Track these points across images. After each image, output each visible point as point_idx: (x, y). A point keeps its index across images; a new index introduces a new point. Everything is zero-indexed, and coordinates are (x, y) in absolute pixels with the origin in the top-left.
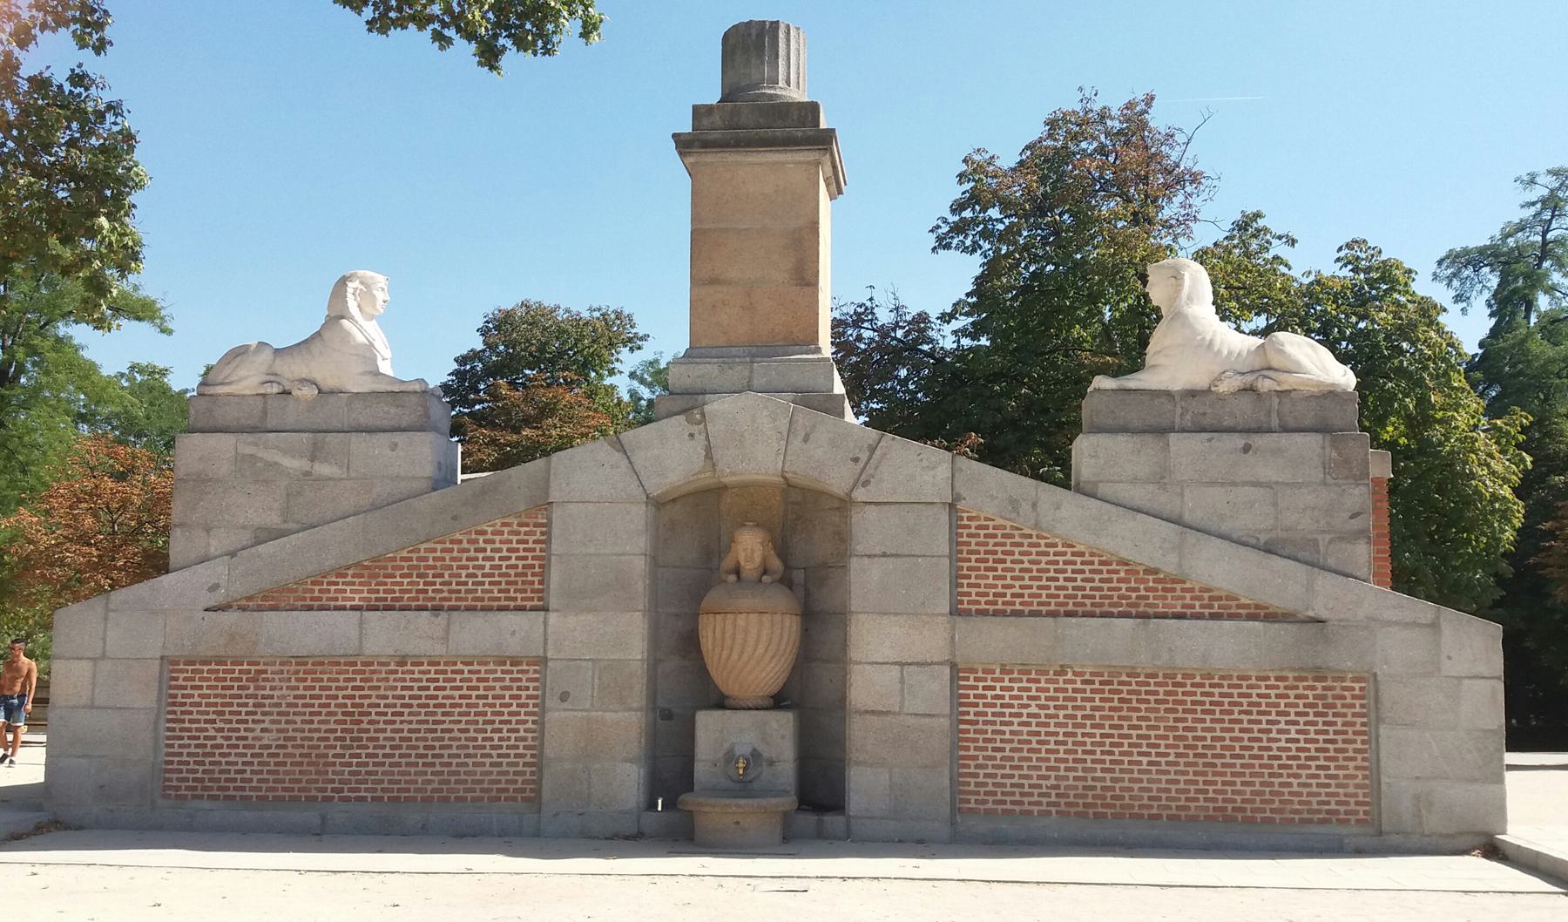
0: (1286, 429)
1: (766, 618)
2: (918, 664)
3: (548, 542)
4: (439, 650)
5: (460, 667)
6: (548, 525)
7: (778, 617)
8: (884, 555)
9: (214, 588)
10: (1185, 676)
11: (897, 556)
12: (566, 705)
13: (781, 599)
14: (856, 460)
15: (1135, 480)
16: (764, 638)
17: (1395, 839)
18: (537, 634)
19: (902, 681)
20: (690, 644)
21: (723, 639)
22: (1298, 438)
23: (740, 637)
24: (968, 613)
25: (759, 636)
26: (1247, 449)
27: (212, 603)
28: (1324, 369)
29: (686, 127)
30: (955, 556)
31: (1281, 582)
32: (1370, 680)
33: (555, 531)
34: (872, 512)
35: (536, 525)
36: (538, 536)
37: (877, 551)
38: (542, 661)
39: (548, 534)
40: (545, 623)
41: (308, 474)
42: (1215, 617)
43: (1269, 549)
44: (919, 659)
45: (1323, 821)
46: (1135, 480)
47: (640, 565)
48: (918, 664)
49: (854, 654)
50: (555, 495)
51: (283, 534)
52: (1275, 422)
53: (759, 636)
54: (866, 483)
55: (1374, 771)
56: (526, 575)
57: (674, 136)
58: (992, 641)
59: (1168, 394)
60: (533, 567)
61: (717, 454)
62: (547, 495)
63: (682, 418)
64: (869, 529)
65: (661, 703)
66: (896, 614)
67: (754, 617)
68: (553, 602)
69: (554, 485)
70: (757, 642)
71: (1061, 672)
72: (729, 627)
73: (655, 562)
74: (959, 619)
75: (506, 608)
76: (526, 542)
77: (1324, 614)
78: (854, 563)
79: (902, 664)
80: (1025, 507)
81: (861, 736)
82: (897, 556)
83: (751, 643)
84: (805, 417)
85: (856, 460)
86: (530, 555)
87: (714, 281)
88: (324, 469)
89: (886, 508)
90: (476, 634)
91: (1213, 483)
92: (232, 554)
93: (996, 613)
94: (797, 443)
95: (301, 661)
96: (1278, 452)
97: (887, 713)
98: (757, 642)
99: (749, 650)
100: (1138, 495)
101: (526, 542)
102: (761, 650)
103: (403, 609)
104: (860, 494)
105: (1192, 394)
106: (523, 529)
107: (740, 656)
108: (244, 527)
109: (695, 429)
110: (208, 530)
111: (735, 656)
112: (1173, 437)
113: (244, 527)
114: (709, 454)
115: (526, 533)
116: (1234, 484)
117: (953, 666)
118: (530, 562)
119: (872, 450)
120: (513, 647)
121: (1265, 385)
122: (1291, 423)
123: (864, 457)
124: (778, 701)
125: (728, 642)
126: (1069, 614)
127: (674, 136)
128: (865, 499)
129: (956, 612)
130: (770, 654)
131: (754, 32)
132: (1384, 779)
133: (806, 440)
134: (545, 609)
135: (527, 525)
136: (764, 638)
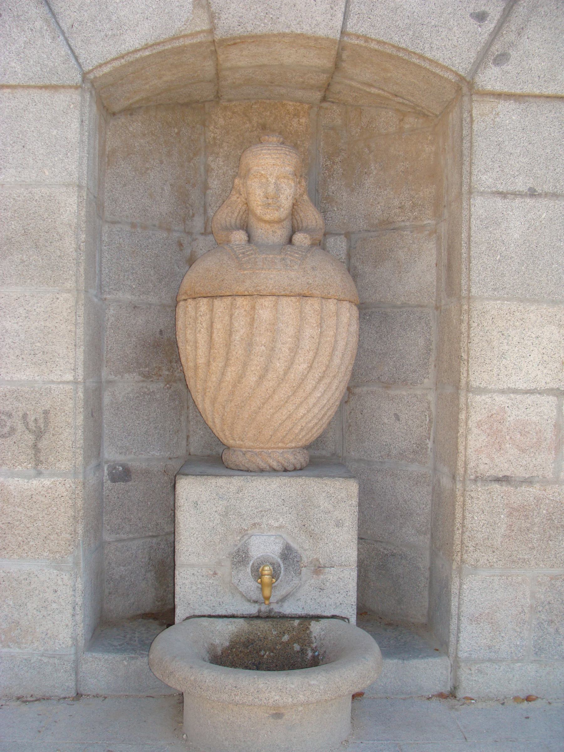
8: (532, 193)
13: (326, 273)
16: (307, 344)
21: (228, 345)
23: (262, 340)
34: (508, 113)
37: (521, 185)
47: (70, 207)
53: (298, 338)
67: (288, 307)
70: (295, 350)
73: (98, 209)
83: (275, 348)
98: (295, 350)
99: (279, 365)
102: (301, 366)
107: (262, 378)
111: (252, 379)
125: (238, 351)
130: (317, 373)
136: (307, 344)
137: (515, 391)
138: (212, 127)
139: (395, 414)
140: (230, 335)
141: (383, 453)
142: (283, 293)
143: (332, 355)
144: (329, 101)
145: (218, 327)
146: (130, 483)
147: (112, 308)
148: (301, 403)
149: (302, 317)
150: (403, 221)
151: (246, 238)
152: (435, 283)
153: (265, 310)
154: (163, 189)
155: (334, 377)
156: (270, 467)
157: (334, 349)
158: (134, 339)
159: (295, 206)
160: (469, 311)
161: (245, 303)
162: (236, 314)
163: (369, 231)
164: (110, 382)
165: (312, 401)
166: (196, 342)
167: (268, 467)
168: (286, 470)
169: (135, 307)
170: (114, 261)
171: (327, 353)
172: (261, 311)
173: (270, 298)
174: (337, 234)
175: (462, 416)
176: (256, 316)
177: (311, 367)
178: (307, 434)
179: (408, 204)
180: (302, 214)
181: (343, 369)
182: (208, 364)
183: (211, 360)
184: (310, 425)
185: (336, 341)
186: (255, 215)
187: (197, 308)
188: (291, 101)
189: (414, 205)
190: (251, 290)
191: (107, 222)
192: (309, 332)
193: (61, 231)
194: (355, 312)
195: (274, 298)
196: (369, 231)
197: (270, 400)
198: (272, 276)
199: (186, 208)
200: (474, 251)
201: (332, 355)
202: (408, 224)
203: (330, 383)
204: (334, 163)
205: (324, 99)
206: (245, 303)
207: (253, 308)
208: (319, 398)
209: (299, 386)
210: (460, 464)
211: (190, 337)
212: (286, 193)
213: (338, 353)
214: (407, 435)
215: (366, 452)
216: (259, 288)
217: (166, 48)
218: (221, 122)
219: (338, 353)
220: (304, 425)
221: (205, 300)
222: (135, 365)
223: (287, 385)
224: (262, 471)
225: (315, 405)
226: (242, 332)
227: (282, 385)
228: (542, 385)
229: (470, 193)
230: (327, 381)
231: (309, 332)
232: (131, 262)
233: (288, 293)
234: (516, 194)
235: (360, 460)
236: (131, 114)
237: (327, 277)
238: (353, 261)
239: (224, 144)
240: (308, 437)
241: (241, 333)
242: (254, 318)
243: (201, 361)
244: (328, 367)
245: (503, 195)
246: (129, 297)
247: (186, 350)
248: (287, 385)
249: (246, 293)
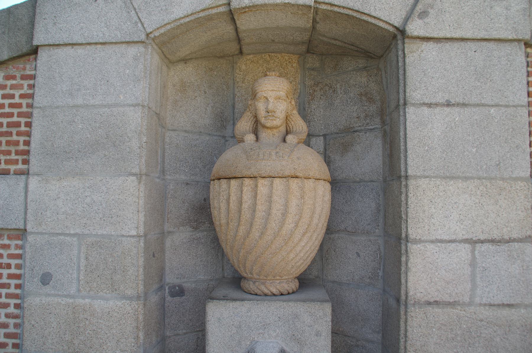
2: (492, 241)
7: (309, 184)
8: (448, 104)
11: (464, 105)
12: (48, 289)
19: (473, 264)
20: (202, 214)
21: (240, 211)
25: (286, 206)
37: (440, 98)
38: (21, 233)
44: (496, 234)
47: (135, 120)
48: (492, 241)
54: (424, 14)
56: (11, 134)
60: (18, 124)
65: (170, 279)
66: (466, 179)
69: (39, 28)
72: (247, 196)
73: (158, 120)
76: (12, 96)
79: (473, 242)
82: (464, 105)
86: (15, 111)
89: (448, 45)
97: (452, 304)
101: (12, 96)
104: (415, 28)
106: (9, 83)
115: (13, 87)
118: (15, 119)
128: (422, 33)
134: (26, 173)
135: (14, 77)
137: (441, 241)
138: (237, 71)
139: (357, 253)
140: (241, 205)
141: (349, 278)
142: (277, 176)
143: (312, 217)
144: (311, 53)
145: (234, 199)
146: (184, 297)
147: (171, 185)
148: (291, 251)
150: (360, 126)
151: (255, 139)
152: (382, 166)
154: (206, 109)
155: (314, 231)
156: (271, 292)
157: (313, 213)
158: (187, 204)
159: (287, 118)
160: (406, 186)
161: (251, 183)
162: (245, 190)
163: (338, 133)
164: (171, 232)
165: (298, 248)
166: (220, 209)
167: (270, 293)
168: (282, 294)
169: (187, 184)
170: (173, 154)
171: (308, 216)
172: (261, 188)
173: (268, 179)
174: (317, 136)
175: (403, 259)
176: (259, 191)
177: (297, 226)
178: (296, 270)
179: (362, 115)
180: (293, 123)
181: (320, 225)
182: (228, 224)
183: (229, 221)
184: (298, 264)
185: (315, 208)
186: (261, 124)
187: (220, 186)
188: (288, 53)
189: (367, 116)
190: (256, 174)
191: (169, 130)
193: (130, 135)
194: (328, 186)
195: (271, 179)
196: (338, 133)
197: (269, 249)
198: (269, 164)
199: (222, 121)
200: (410, 145)
201: (312, 217)
202: (363, 128)
203: (311, 236)
204: (314, 91)
205: (308, 51)
206: (251, 183)
207: (256, 186)
208: (304, 246)
209: (289, 238)
210: (403, 292)
211: (216, 205)
212: (281, 108)
213: (316, 216)
214: (364, 266)
215: (338, 277)
216: (260, 172)
217: (200, 16)
218: (244, 67)
219: (316, 216)
220: (293, 264)
221: (225, 180)
222: (187, 221)
223: (281, 239)
224: (266, 295)
225: (300, 251)
226: (249, 202)
227: (277, 239)
228: (460, 237)
229: (405, 104)
230: (308, 235)
232: (184, 155)
233: (280, 176)
234: (437, 105)
235: (334, 282)
236: (186, 63)
237: (308, 164)
238: (327, 152)
239: (246, 81)
240: (296, 272)
241: (249, 203)
242: (257, 193)
243: (223, 221)
244: (309, 225)
245: (429, 105)
246: (183, 177)
247: (215, 213)
248: (281, 239)
249: (252, 176)
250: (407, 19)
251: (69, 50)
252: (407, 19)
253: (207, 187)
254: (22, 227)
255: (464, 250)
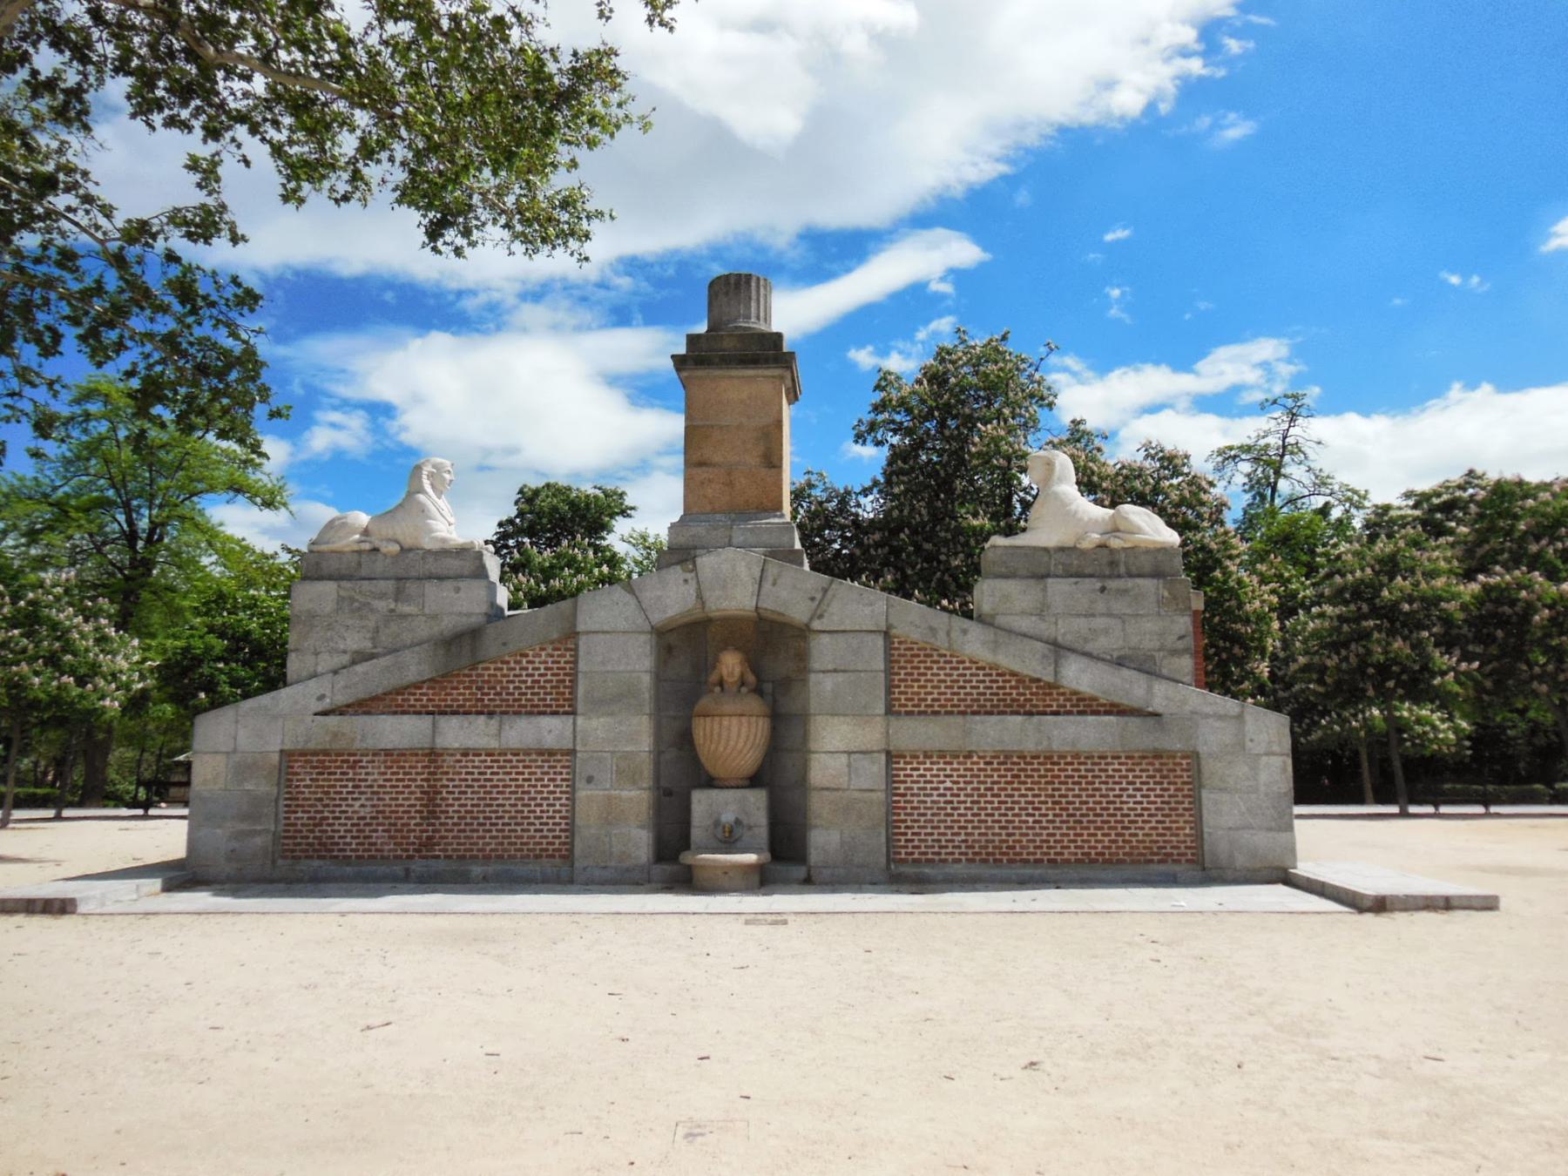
0: (1131, 575)
1: (744, 719)
3: (575, 662)
4: (494, 744)
5: (509, 757)
6: (576, 649)
8: (835, 671)
9: (321, 698)
10: (1060, 757)
12: (592, 786)
13: (754, 704)
14: (813, 599)
15: (1023, 613)
17: (1214, 873)
18: (569, 733)
19: (849, 765)
20: (686, 740)
22: (1139, 581)
23: (725, 734)
24: (899, 713)
26: (1103, 589)
27: (320, 709)
28: (1157, 531)
29: (682, 350)
30: (889, 672)
31: (1132, 687)
32: (1194, 756)
33: (581, 653)
34: (825, 639)
35: (567, 650)
36: (568, 658)
37: (830, 667)
38: (572, 752)
39: (576, 656)
40: (574, 724)
41: (392, 611)
42: (1080, 713)
43: (1120, 662)
44: (863, 748)
45: (1160, 862)
46: (1023, 613)
47: (646, 680)
49: (813, 746)
50: (580, 627)
51: (372, 656)
52: (1122, 569)
54: (821, 617)
55: (1198, 823)
57: (673, 357)
58: (915, 733)
59: (1046, 550)
61: (707, 594)
62: (575, 626)
63: (678, 568)
64: (824, 651)
65: (664, 784)
67: (735, 720)
68: (580, 708)
69: (580, 618)
71: (969, 756)
72: (716, 727)
73: (659, 677)
74: (892, 718)
75: (544, 713)
77: (1160, 710)
78: (813, 677)
79: (849, 753)
80: (942, 635)
81: (819, 806)
83: (734, 736)
84: (774, 567)
85: (813, 599)
87: (701, 464)
88: (405, 608)
90: (522, 732)
91: (1078, 615)
92: (335, 672)
93: (920, 713)
94: (767, 586)
95: (388, 753)
96: (1123, 592)
97: (837, 790)
99: (732, 743)
100: (1025, 624)
102: (741, 745)
103: (466, 713)
105: (1062, 549)
108: (345, 652)
109: (689, 576)
110: (317, 654)
112: (1050, 580)
113: (345, 652)
114: (700, 596)
116: (1093, 615)
117: (888, 753)
119: (825, 591)
120: (550, 742)
121: (1115, 543)
122: (1134, 570)
123: (819, 596)
124: (754, 781)
126: (974, 713)
127: (673, 357)
129: (889, 711)
131: (732, 281)
132: (1206, 830)
133: (774, 584)
134: (574, 713)
136: (743, 735)
149: (741, 724)
153: (726, 722)
192: (744, 730)
231: (744, 730)
250: (811, 619)
251: (602, 636)
252: (811, 619)
253: (690, 719)
254: (570, 746)
255: (844, 758)
